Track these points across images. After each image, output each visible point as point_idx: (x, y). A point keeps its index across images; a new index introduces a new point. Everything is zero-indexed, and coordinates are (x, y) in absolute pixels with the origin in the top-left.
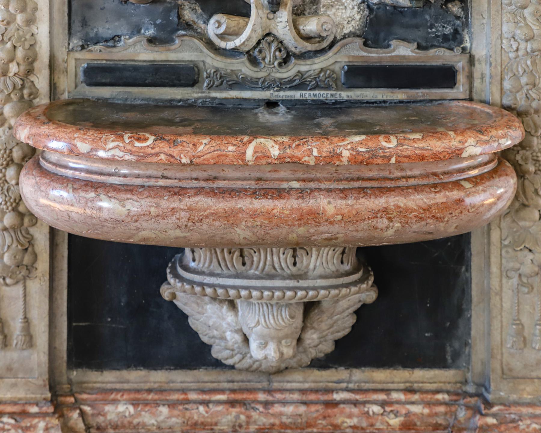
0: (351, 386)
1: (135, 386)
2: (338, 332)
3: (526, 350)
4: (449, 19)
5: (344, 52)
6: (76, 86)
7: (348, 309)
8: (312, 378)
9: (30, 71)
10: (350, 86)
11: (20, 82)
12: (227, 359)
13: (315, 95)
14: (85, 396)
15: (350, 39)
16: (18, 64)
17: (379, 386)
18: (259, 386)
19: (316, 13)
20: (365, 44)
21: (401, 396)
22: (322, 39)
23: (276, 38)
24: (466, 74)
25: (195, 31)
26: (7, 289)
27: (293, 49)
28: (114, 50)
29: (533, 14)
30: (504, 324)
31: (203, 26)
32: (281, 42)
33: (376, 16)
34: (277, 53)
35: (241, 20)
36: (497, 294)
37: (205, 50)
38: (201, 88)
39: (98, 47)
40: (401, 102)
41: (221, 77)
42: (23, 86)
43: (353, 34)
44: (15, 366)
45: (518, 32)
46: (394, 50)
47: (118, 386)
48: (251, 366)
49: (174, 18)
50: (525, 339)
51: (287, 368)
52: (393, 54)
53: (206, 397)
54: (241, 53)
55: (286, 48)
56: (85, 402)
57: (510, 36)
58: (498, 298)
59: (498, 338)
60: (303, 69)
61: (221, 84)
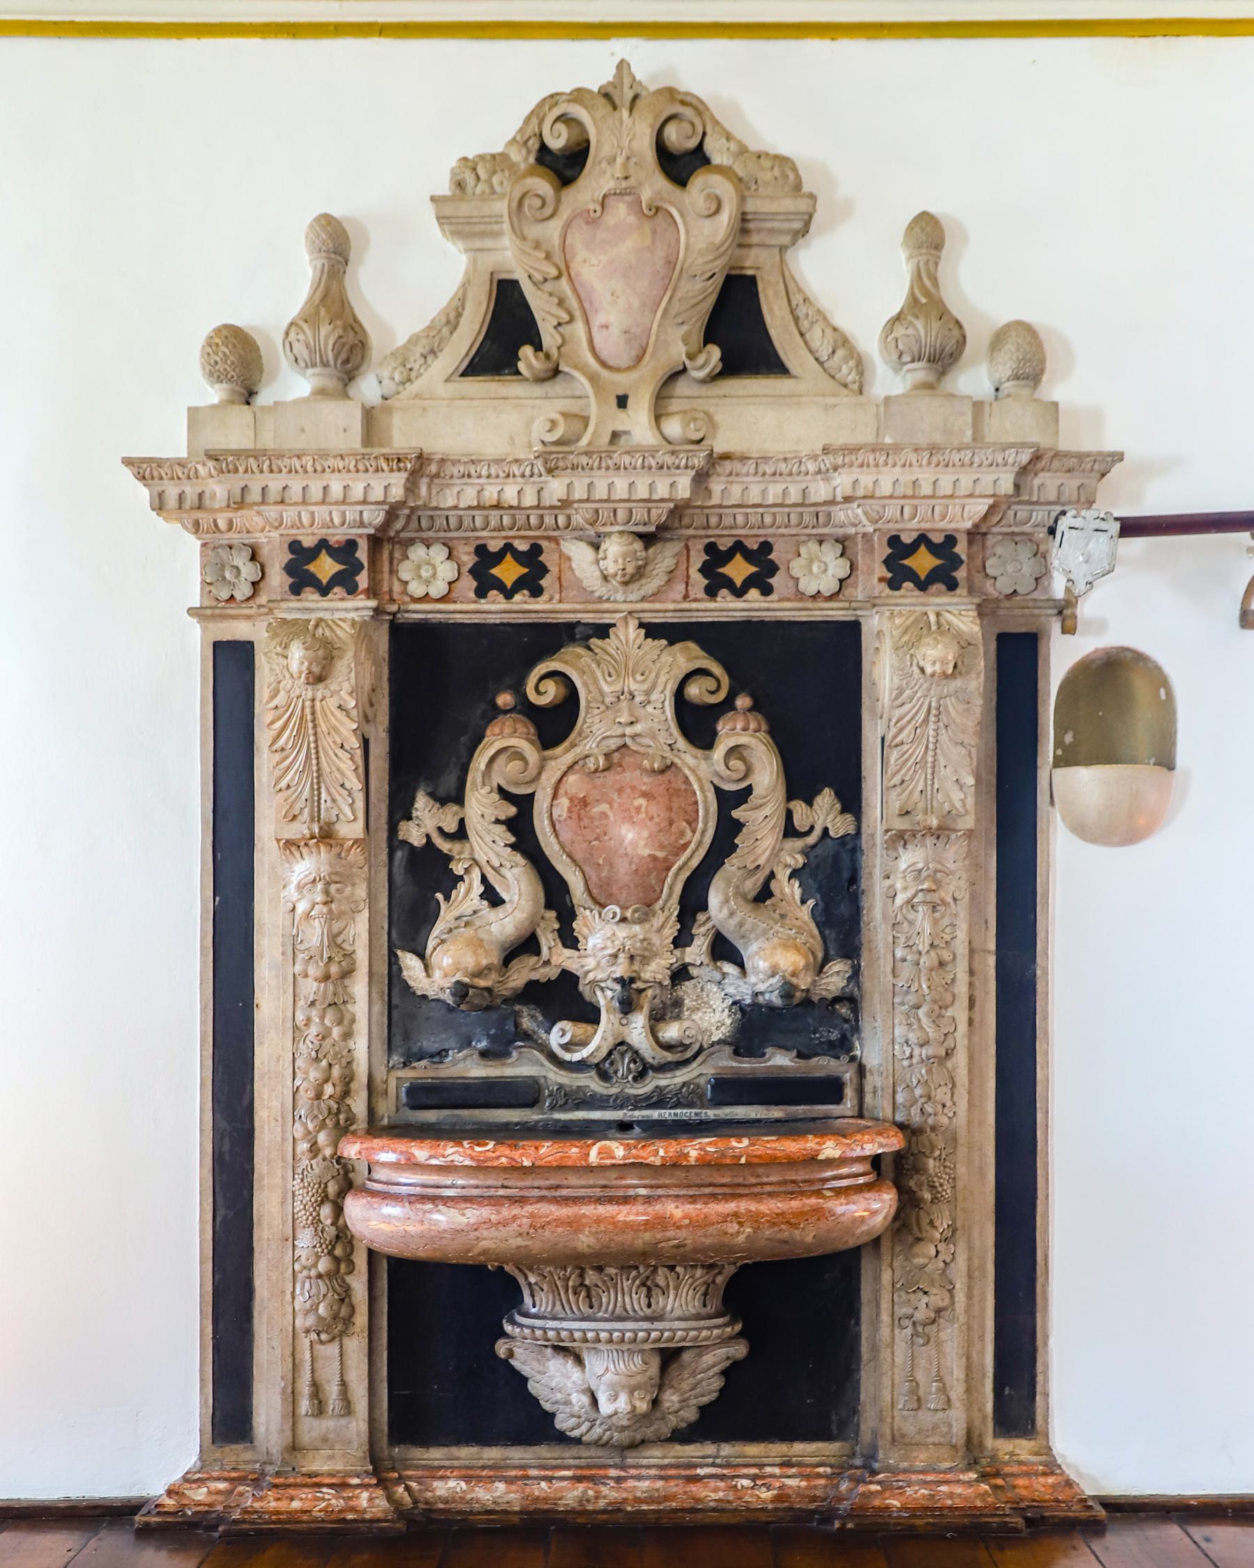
0: (718, 1461)
1: (467, 1463)
2: (703, 1396)
3: (920, 1412)
4: (836, 1022)
5: (710, 1062)
6: (397, 1110)
7: (714, 1366)
8: (673, 1453)
9: (346, 1093)
10: (717, 1103)
11: (335, 1106)
12: (573, 1429)
13: (676, 1115)
14: (410, 1473)
15: (717, 1047)
16: (334, 1085)
17: (752, 1461)
18: (610, 1462)
19: (678, 1017)
20: (736, 1053)
21: (777, 1471)
22: (686, 1047)
23: (630, 1047)
24: (854, 1086)
25: (535, 1042)
26: (322, 1347)
27: (651, 1060)
28: (441, 1066)
29: (928, 1015)
30: (896, 1382)
31: (544, 1036)
32: (636, 1052)
33: (749, 1020)
34: (632, 1065)
35: (589, 1028)
36: (887, 1346)
37: (547, 1063)
38: (542, 1108)
39: (424, 1063)
40: (778, 1121)
41: (566, 1095)
42: (339, 1111)
43: (720, 1042)
44: (332, 1436)
45: (911, 1035)
46: (769, 1059)
47: (447, 1463)
48: (600, 1438)
49: (510, 1027)
50: (919, 1400)
51: (643, 1442)
52: (769, 1064)
53: (549, 1473)
54: (590, 1066)
55: (642, 1059)
56: (410, 1478)
57: (902, 1041)
58: (889, 1350)
59: (889, 1398)
60: (663, 1083)
61: (566, 1103)
